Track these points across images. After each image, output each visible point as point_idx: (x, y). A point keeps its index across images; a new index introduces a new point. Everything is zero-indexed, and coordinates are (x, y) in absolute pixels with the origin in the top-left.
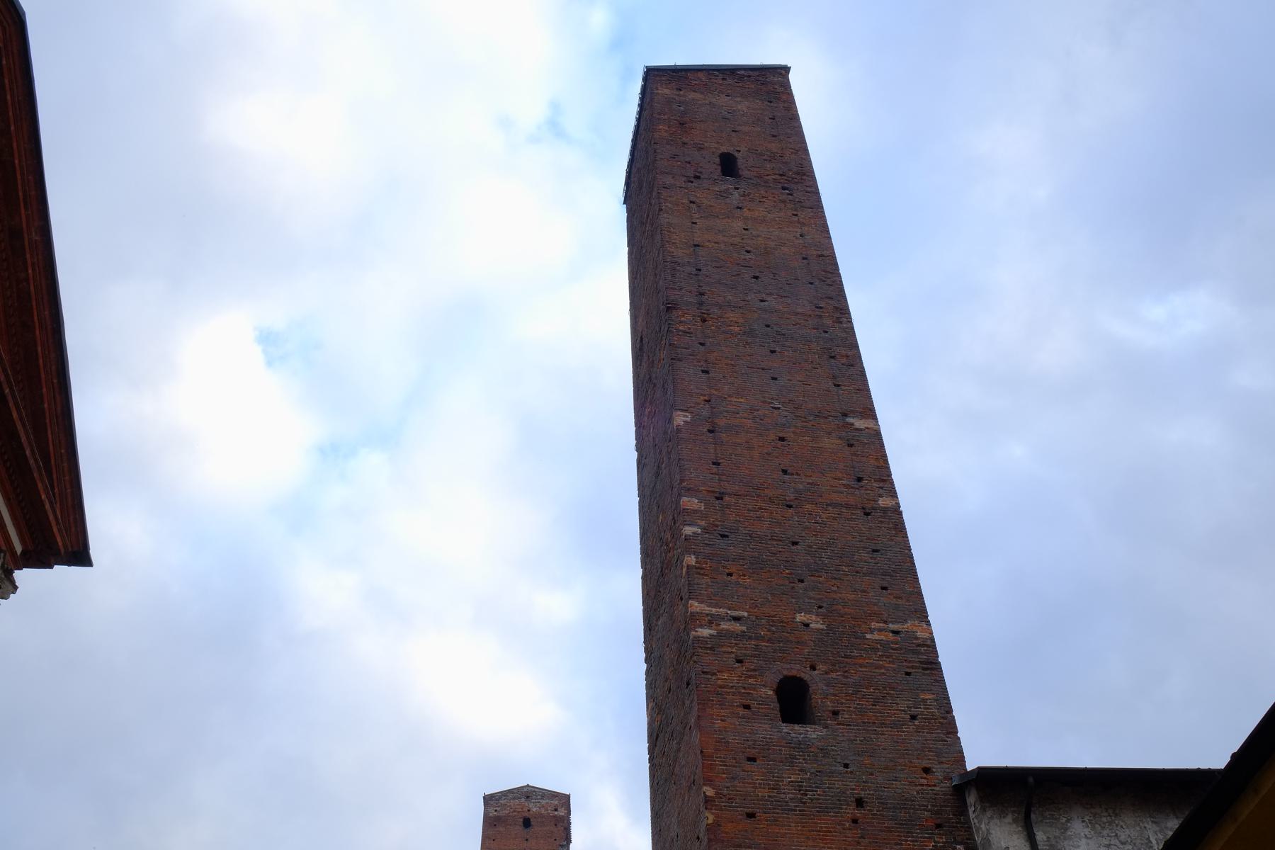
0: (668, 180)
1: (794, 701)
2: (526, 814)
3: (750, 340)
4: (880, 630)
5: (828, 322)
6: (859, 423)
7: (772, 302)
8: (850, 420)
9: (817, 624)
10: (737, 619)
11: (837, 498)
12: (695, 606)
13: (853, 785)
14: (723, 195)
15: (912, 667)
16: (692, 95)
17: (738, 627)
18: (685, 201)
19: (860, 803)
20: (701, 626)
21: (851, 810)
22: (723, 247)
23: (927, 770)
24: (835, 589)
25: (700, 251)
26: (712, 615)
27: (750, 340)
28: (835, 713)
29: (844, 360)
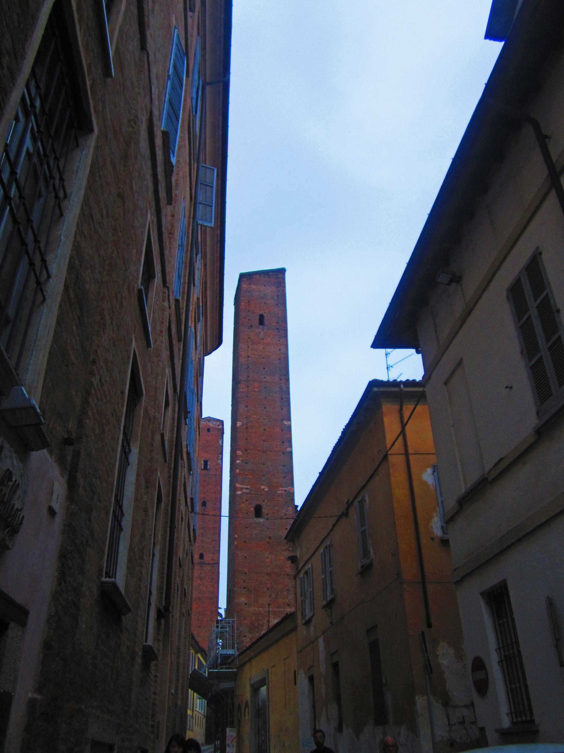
1: (258, 511)
6: (286, 423)
10: (247, 488)
12: (238, 485)
14: (259, 333)
17: (247, 491)
19: (270, 538)
21: (268, 540)
22: (256, 357)
25: (250, 359)
28: (267, 514)
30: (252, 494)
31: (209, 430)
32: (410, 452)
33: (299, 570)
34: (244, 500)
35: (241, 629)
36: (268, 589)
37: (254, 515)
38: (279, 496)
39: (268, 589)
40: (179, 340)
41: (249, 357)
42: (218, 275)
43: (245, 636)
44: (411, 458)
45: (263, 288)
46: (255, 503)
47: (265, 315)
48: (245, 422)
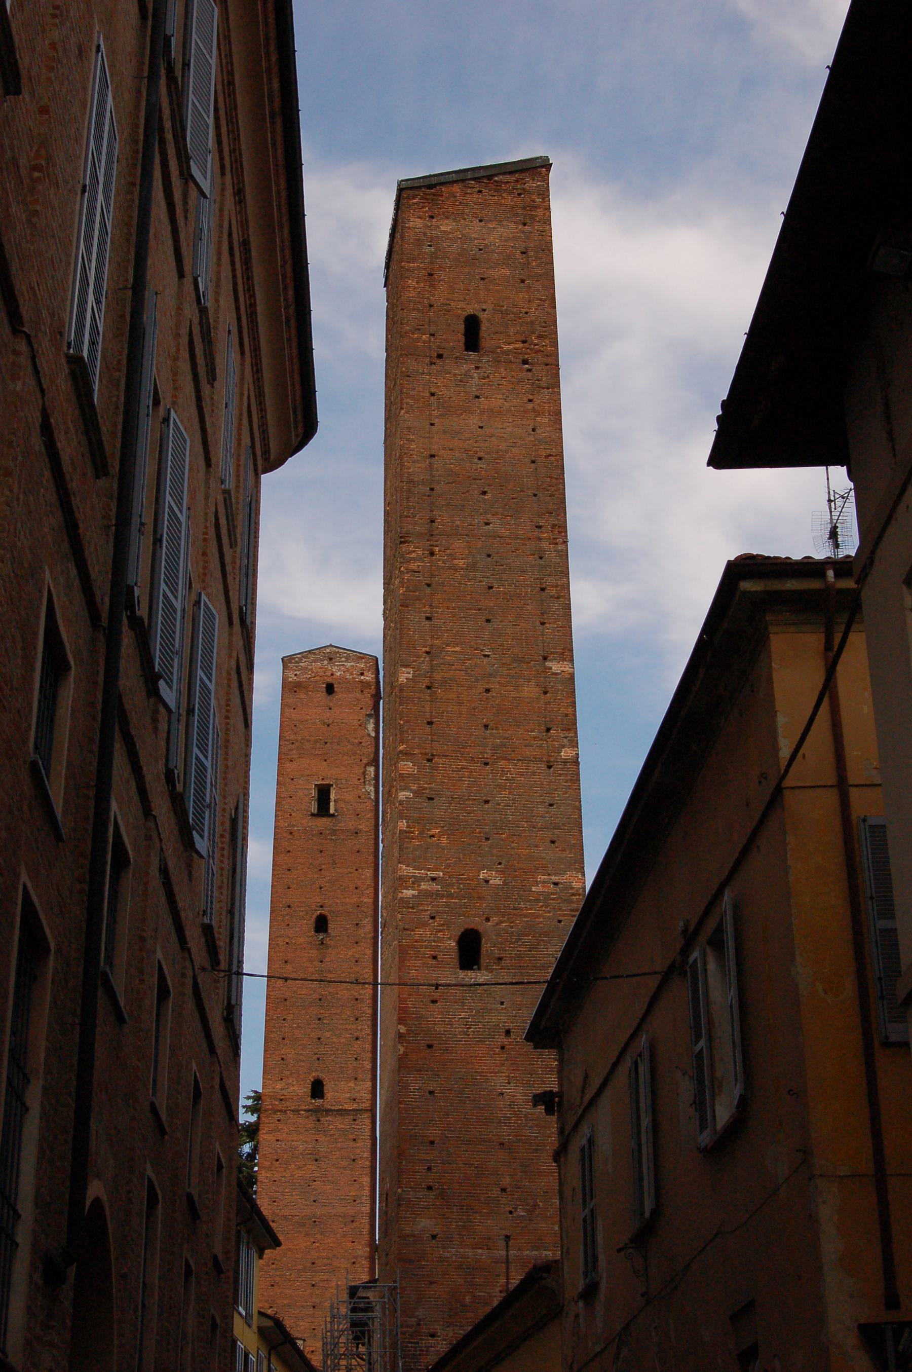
2: (330, 680)
4: (544, 882)
5: (545, 545)
6: (556, 667)
7: (496, 524)
8: (548, 664)
9: (496, 881)
10: (433, 879)
11: (528, 752)
12: (405, 870)
13: (504, 1019)
14: (463, 381)
15: (564, 915)
18: (428, 395)
20: (406, 888)
21: (501, 1039)
22: (457, 454)
24: (513, 845)
26: (415, 877)
28: (500, 959)
29: (554, 592)
30: (450, 896)
31: (330, 689)
32: (851, 782)
33: (566, 1133)
34: (425, 916)
35: (420, 1313)
36: (504, 1190)
37: (456, 962)
38: (537, 900)
39: (504, 1190)
40: (100, 468)
41: (432, 456)
42: (285, 219)
43: (433, 1335)
44: (854, 793)
45: (475, 229)
46: (461, 924)
47: (483, 317)
48: (425, 667)
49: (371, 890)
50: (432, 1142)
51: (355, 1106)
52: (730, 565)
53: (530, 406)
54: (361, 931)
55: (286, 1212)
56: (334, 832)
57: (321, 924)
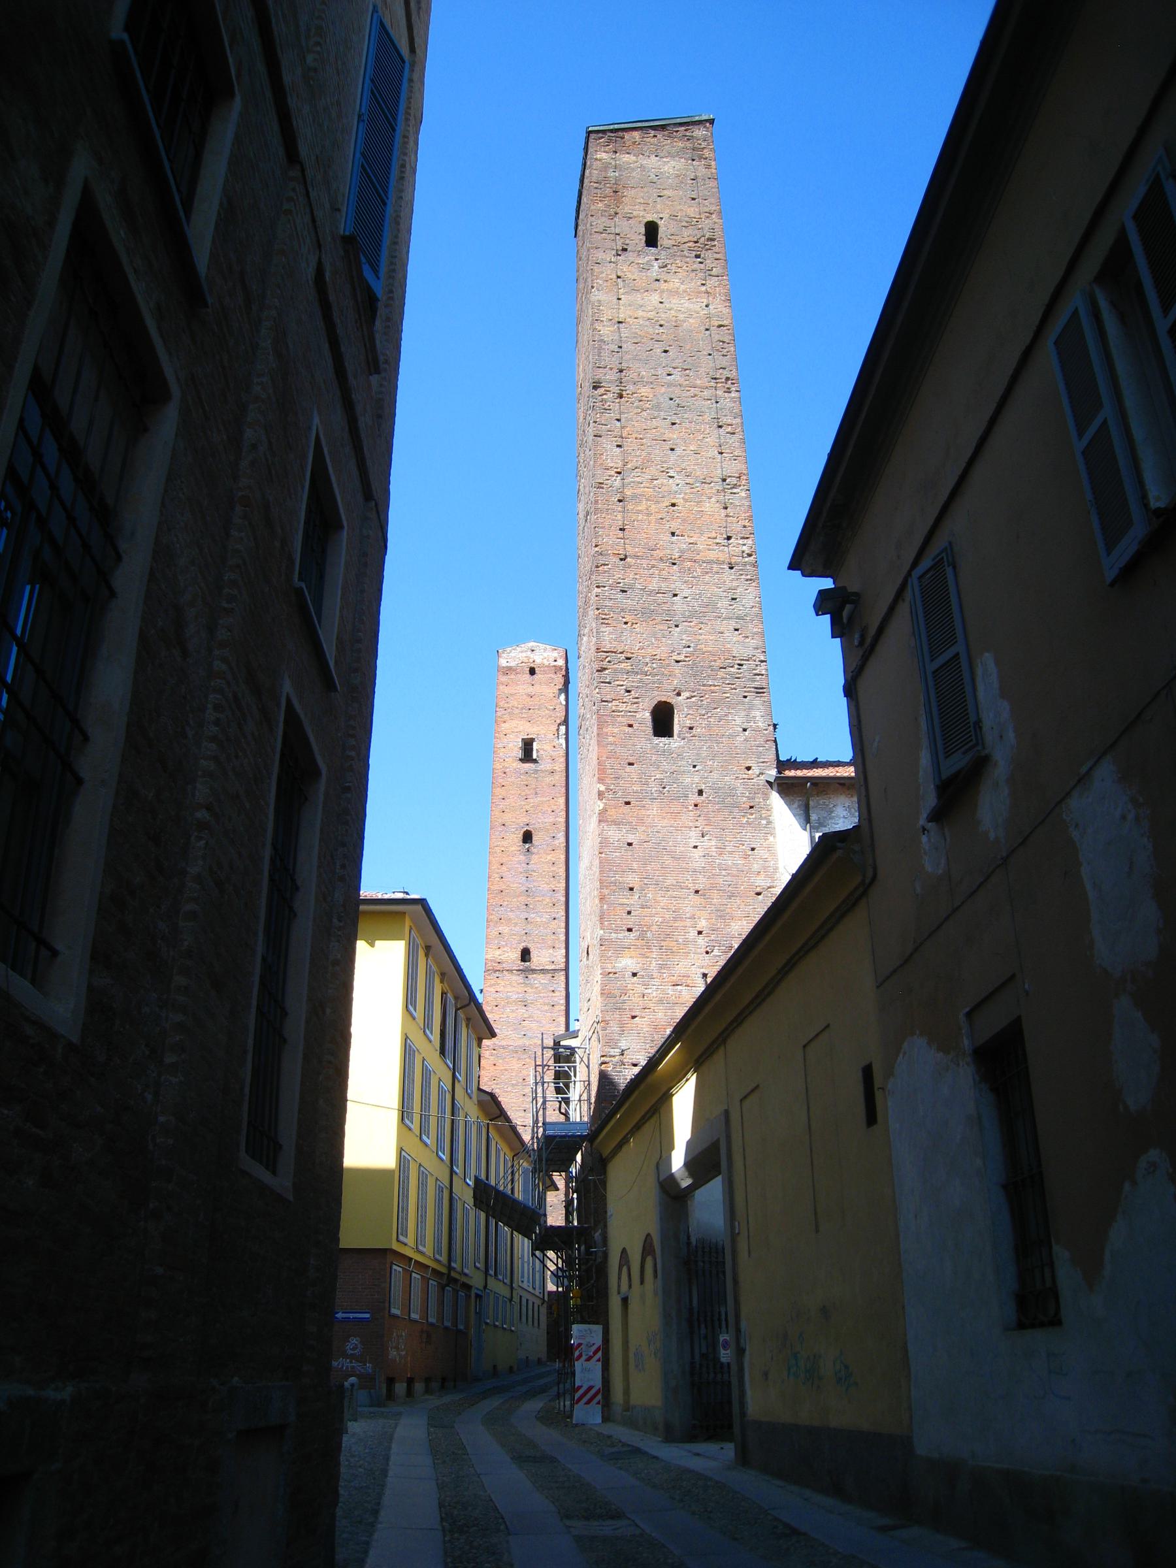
0: (600, 255)
3: (656, 414)
7: (677, 377)
11: (712, 555)
14: (645, 268)
16: (626, 158)
23: (749, 768)
27: (656, 414)
29: (729, 429)
31: (532, 671)
35: (623, 1044)
37: (650, 730)
47: (661, 223)
49: (564, 813)
50: (631, 889)
51: (553, 967)
52: (814, 606)
53: (703, 288)
54: (556, 842)
55: (504, 1043)
56: (536, 771)
57: (527, 837)
